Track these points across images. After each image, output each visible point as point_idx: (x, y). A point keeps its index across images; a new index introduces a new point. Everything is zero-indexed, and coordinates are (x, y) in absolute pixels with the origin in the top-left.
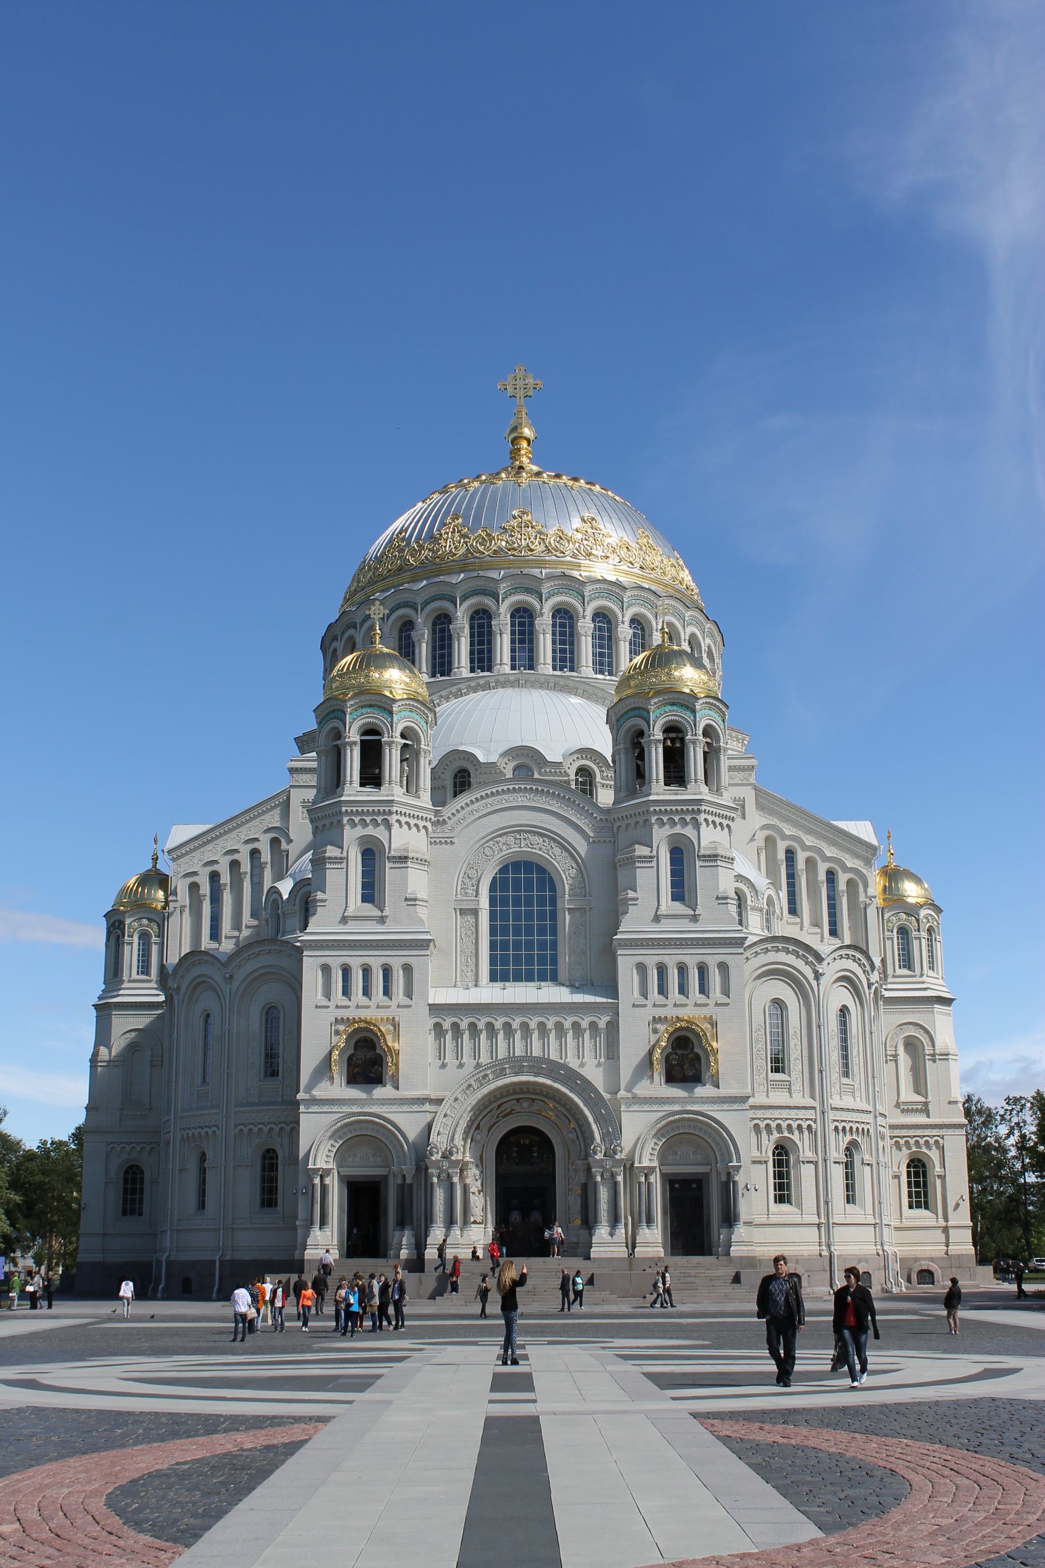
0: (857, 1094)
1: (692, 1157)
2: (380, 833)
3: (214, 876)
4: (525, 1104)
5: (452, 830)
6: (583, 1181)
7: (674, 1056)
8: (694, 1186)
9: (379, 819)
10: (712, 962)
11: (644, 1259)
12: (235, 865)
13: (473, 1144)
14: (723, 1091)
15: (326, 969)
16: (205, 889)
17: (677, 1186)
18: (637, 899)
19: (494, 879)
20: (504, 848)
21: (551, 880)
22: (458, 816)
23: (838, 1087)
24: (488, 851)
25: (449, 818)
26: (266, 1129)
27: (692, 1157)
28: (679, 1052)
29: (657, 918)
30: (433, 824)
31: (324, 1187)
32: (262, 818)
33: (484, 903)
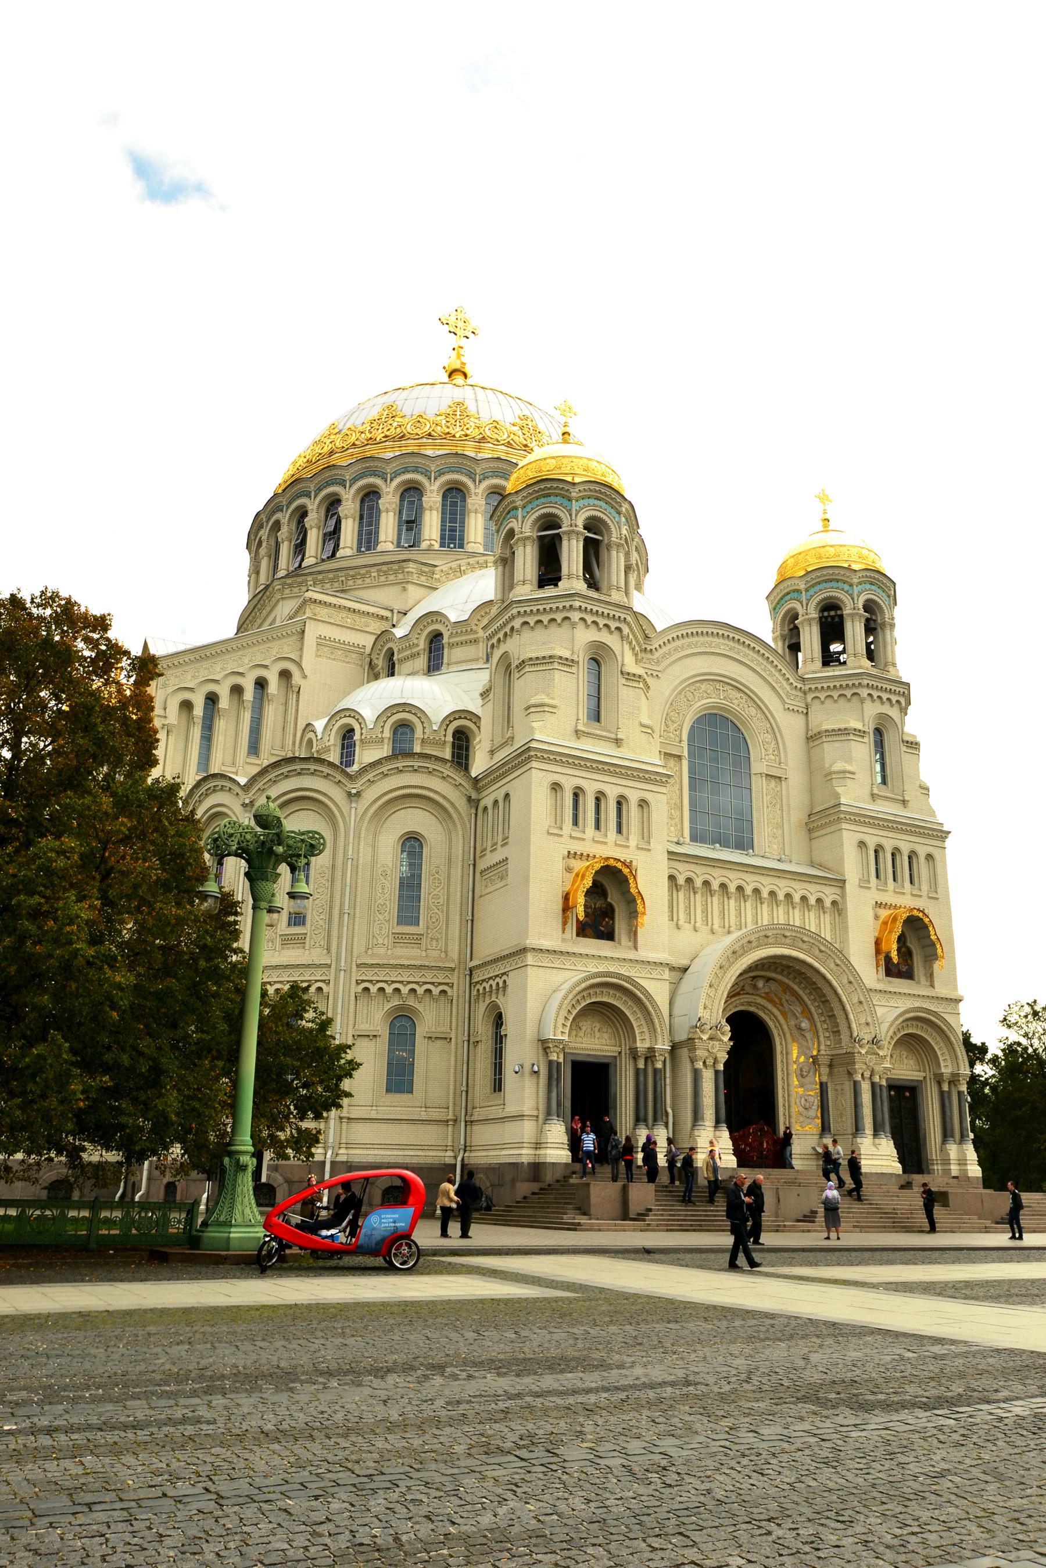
2: (612, 640)
3: (212, 699)
4: (760, 984)
5: (658, 662)
6: (824, 1079)
9: (613, 625)
12: (237, 690)
14: (941, 990)
15: (556, 787)
16: (199, 711)
17: (892, 1093)
18: (853, 773)
20: (705, 695)
24: (689, 694)
26: (405, 990)
29: (873, 796)
32: (270, 645)
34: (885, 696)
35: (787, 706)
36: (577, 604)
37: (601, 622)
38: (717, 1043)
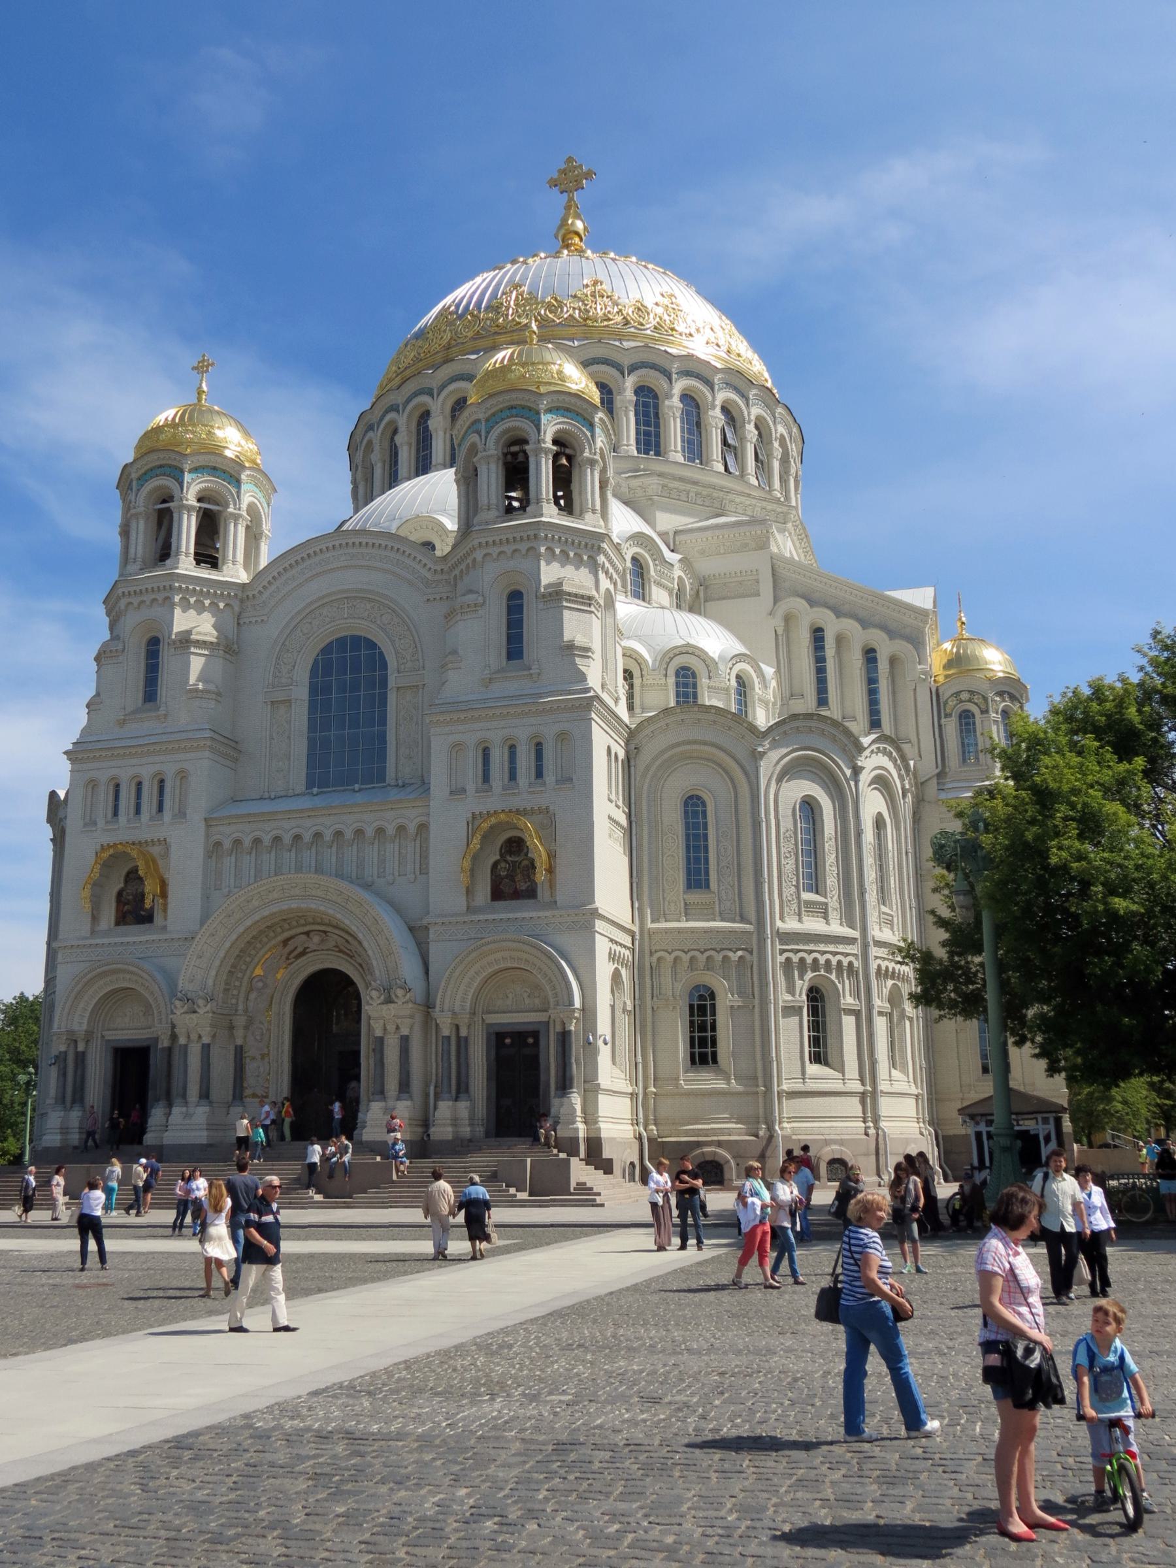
0: (834, 915)
1: (527, 1001)
4: (316, 939)
7: (503, 865)
8: (531, 1040)
10: (549, 733)
11: (441, 1142)
13: (253, 996)
17: (508, 1041)
19: (316, 662)
21: (381, 653)
22: (273, 588)
23: (795, 906)
25: (260, 592)
27: (527, 1001)
28: (509, 858)
30: (242, 601)
31: (81, 1058)
33: (301, 693)
34: (508, 549)
35: (425, 598)
36: (120, 591)
37: (147, 598)
38: (194, 1016)
